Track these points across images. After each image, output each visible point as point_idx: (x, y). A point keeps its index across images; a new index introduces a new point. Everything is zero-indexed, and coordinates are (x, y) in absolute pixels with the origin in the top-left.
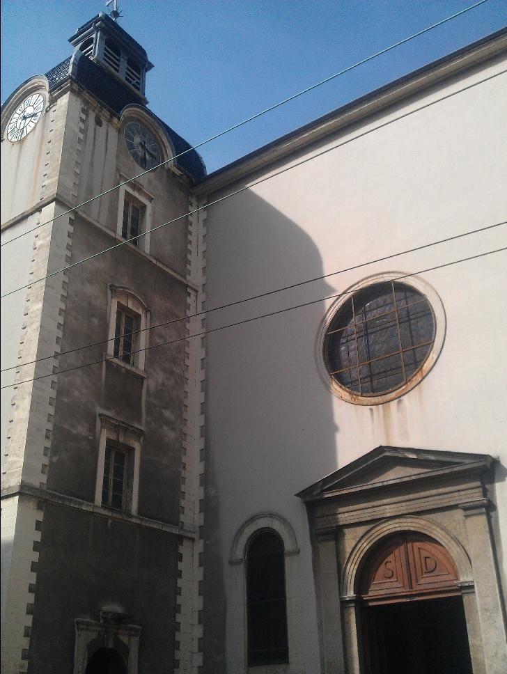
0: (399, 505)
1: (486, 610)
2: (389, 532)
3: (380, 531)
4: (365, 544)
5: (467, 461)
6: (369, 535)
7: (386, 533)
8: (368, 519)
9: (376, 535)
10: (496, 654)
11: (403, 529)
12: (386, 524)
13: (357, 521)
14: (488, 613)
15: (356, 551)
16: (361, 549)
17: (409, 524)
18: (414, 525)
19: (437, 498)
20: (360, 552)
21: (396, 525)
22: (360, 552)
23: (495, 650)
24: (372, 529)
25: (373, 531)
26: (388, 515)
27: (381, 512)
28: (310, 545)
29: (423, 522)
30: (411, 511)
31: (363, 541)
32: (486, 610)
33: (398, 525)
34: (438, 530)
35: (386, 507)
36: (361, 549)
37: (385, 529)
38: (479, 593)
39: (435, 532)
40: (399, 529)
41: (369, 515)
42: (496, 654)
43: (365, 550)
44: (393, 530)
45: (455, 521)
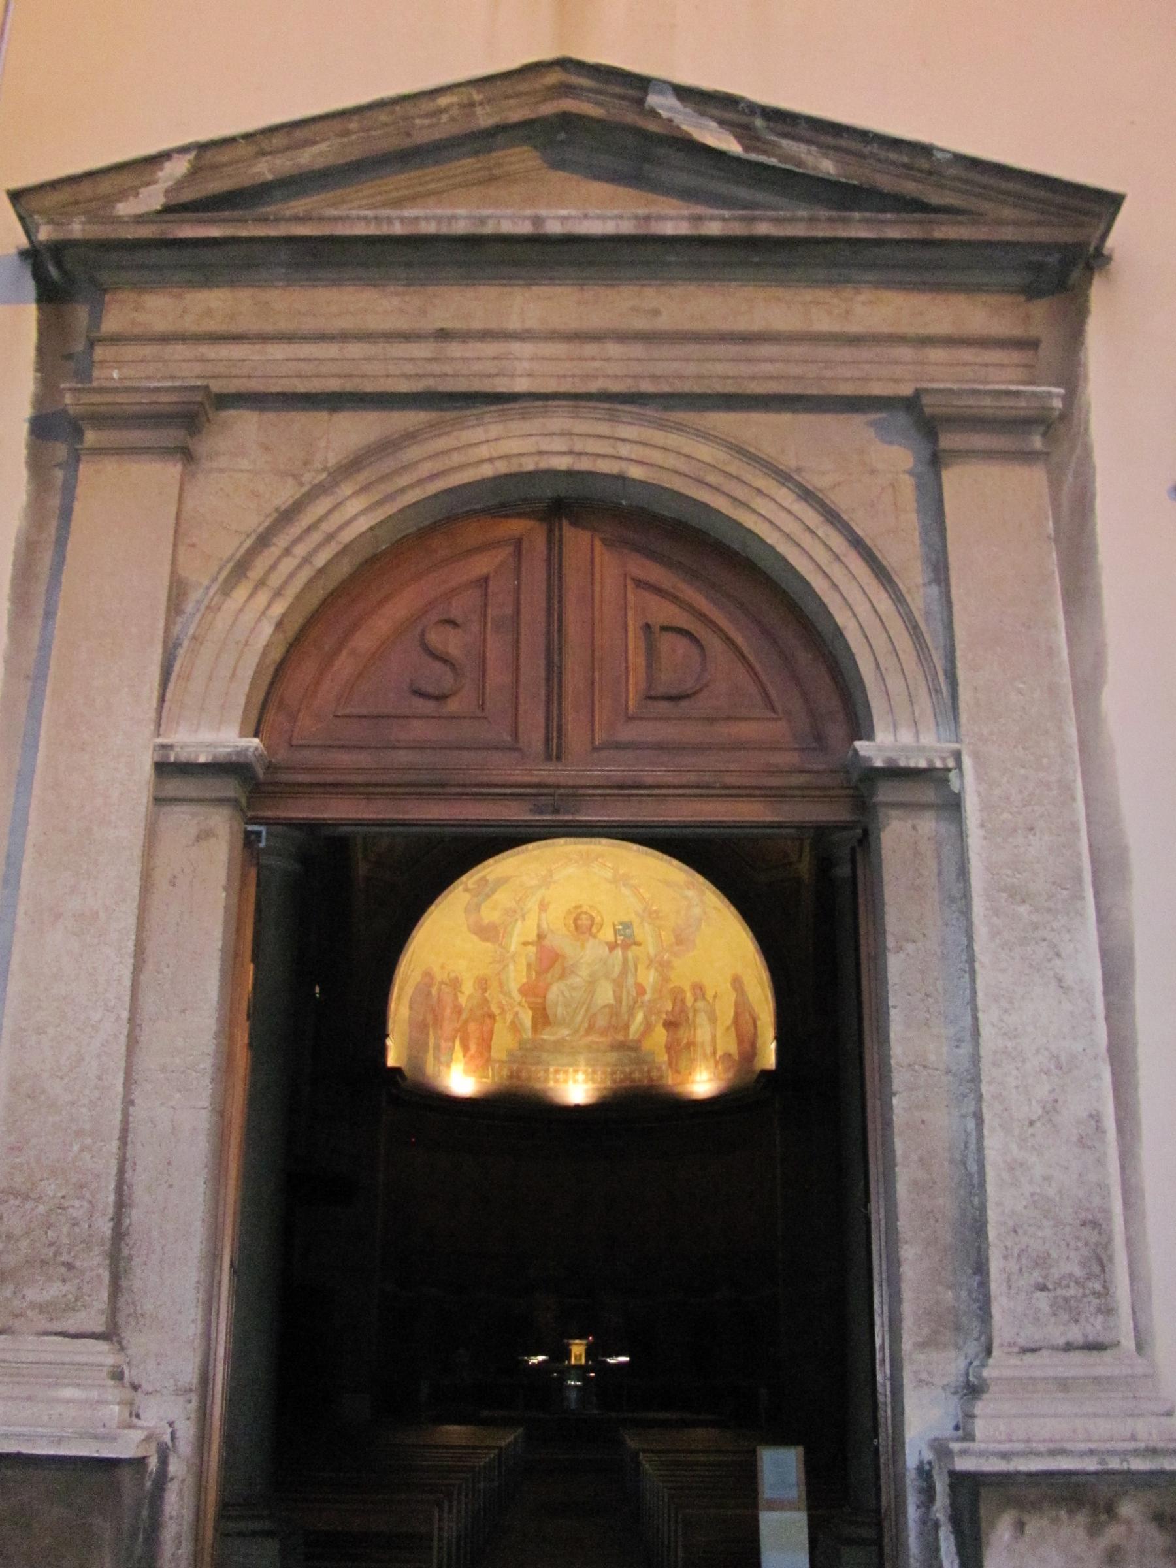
0: (591, 349)
1: (1018, 895)
2: (502, 468)
3: (456, 459)
4: (354, 507)
5: (1007, 212)
6: (387, 465)
7: (487, 471)
8: (404, 387)
9: (426, 468)
10: (1052, 1108)
11: (584, 465)
12: (495, 430)
13: (334, 385)
14: (1023, 909)
15: (295, 530)
16: (327, 527)
17: (624, 450)
18: (657, 457)
19: (797, 351)
20: (317, 537)
21: (546, 445)
22: (317, 537)
23: (1042, 1090)
24: (411, 437)
25: (413, 452)
26: (521, 385)
27: (489, 367)
28: (24, 473)
29: (705, 452)
30: (647, 387)
31: (347, 489)
32: (1018, 895)
33: (559, 445)
34: (785, 496)
35: (516, 347)
36: (327, 527)
37: (484, 451)
38: (987, 807)
39: (759, 504)
40: (562, 463)
41: (409, 368)
42: (1052, 1108)
43: (347, 536)
44: (529, 465)
45: (873, 472)
